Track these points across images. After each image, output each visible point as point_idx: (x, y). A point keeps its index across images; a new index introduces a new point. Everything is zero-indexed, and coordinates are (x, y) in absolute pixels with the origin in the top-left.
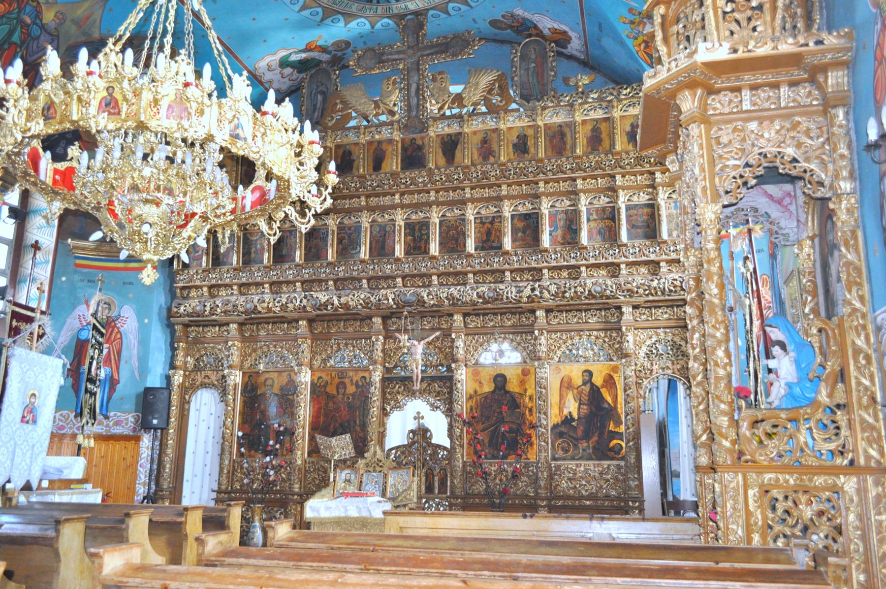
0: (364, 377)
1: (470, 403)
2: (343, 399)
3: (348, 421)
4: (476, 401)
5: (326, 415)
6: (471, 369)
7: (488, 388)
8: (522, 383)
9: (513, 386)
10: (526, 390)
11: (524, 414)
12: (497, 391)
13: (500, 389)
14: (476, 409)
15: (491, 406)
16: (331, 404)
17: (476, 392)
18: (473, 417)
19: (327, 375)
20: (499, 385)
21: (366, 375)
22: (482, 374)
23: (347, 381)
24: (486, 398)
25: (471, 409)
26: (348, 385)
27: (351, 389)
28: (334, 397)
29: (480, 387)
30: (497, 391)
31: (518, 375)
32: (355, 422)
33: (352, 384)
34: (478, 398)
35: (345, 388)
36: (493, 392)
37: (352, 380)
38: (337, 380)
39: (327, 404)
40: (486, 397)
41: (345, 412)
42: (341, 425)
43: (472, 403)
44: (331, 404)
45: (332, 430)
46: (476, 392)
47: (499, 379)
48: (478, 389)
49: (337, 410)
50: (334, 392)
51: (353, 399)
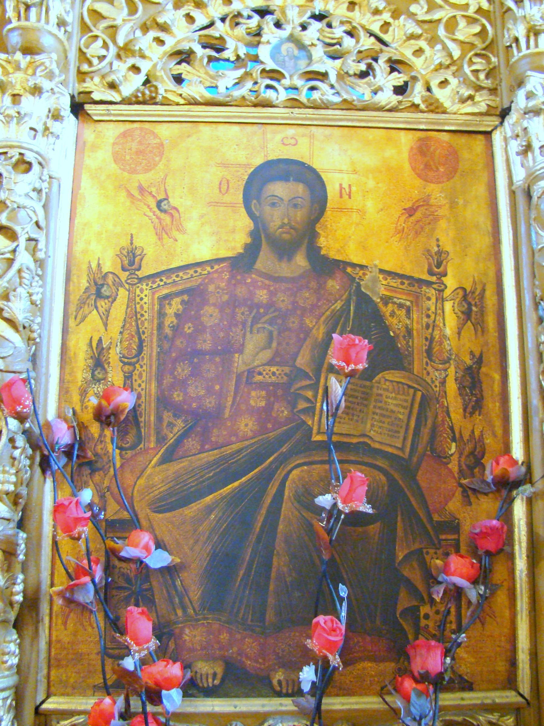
1: (90, 328)
4: (133, 314)
6: (111, 132)
7: (209, 234)
8: (417, 215)
9: (365, 232)
10: (438, 263)
11: (427, 403)
12: (265, 261)
13: (284, 250)
14: (130, 362)
15: (227, 350)
17: (131, 259)
18: (105, 417)
20: (275, 219)
22: (176, 159)
24: (195, 296)
25: (98, 362)
29: (162, 232)
30: (265, 261)
31: (389, 172)
34: (146, 295)
36: (242, 263)
40: (192, 289)
43: (108, 326)
46: (131, 259)
47: (279, 189)
48: (146, 241)
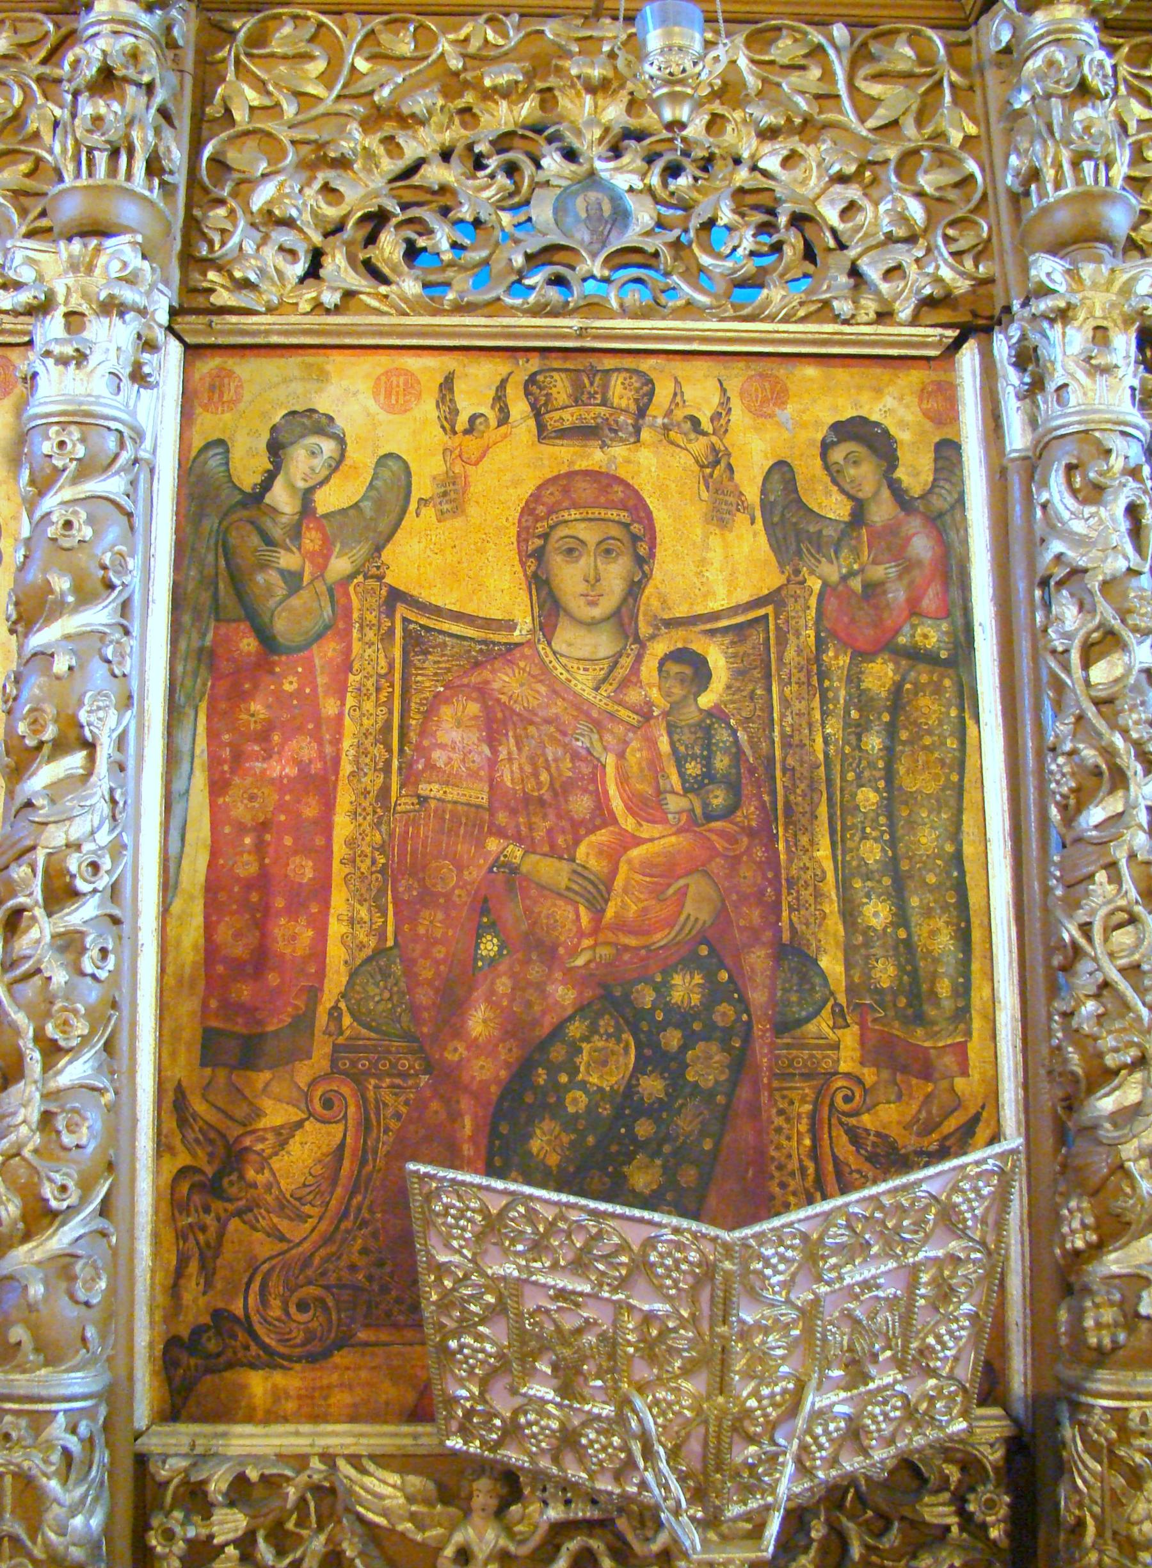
0: (858, 431)
2: (618, 675)
3: (710, 951)
5: (402, 875)
16: (455, 734)
19: (395, 393)
21: (894, 407)
23: (654, 468)
26: (675, 511)
27: (715, 566)
28: (493, 649)
32: (795, 956)
33: (723, 507)
35: (638, 539)
37: (717, 464)
38: (516, 464)
39: (404, 742)
41: (659, 841)
42: (609, 999)
44: (455, 734)
45: (486, 1071)
49: (551, 809)
50: (503, 594)
51: (756, 670)
